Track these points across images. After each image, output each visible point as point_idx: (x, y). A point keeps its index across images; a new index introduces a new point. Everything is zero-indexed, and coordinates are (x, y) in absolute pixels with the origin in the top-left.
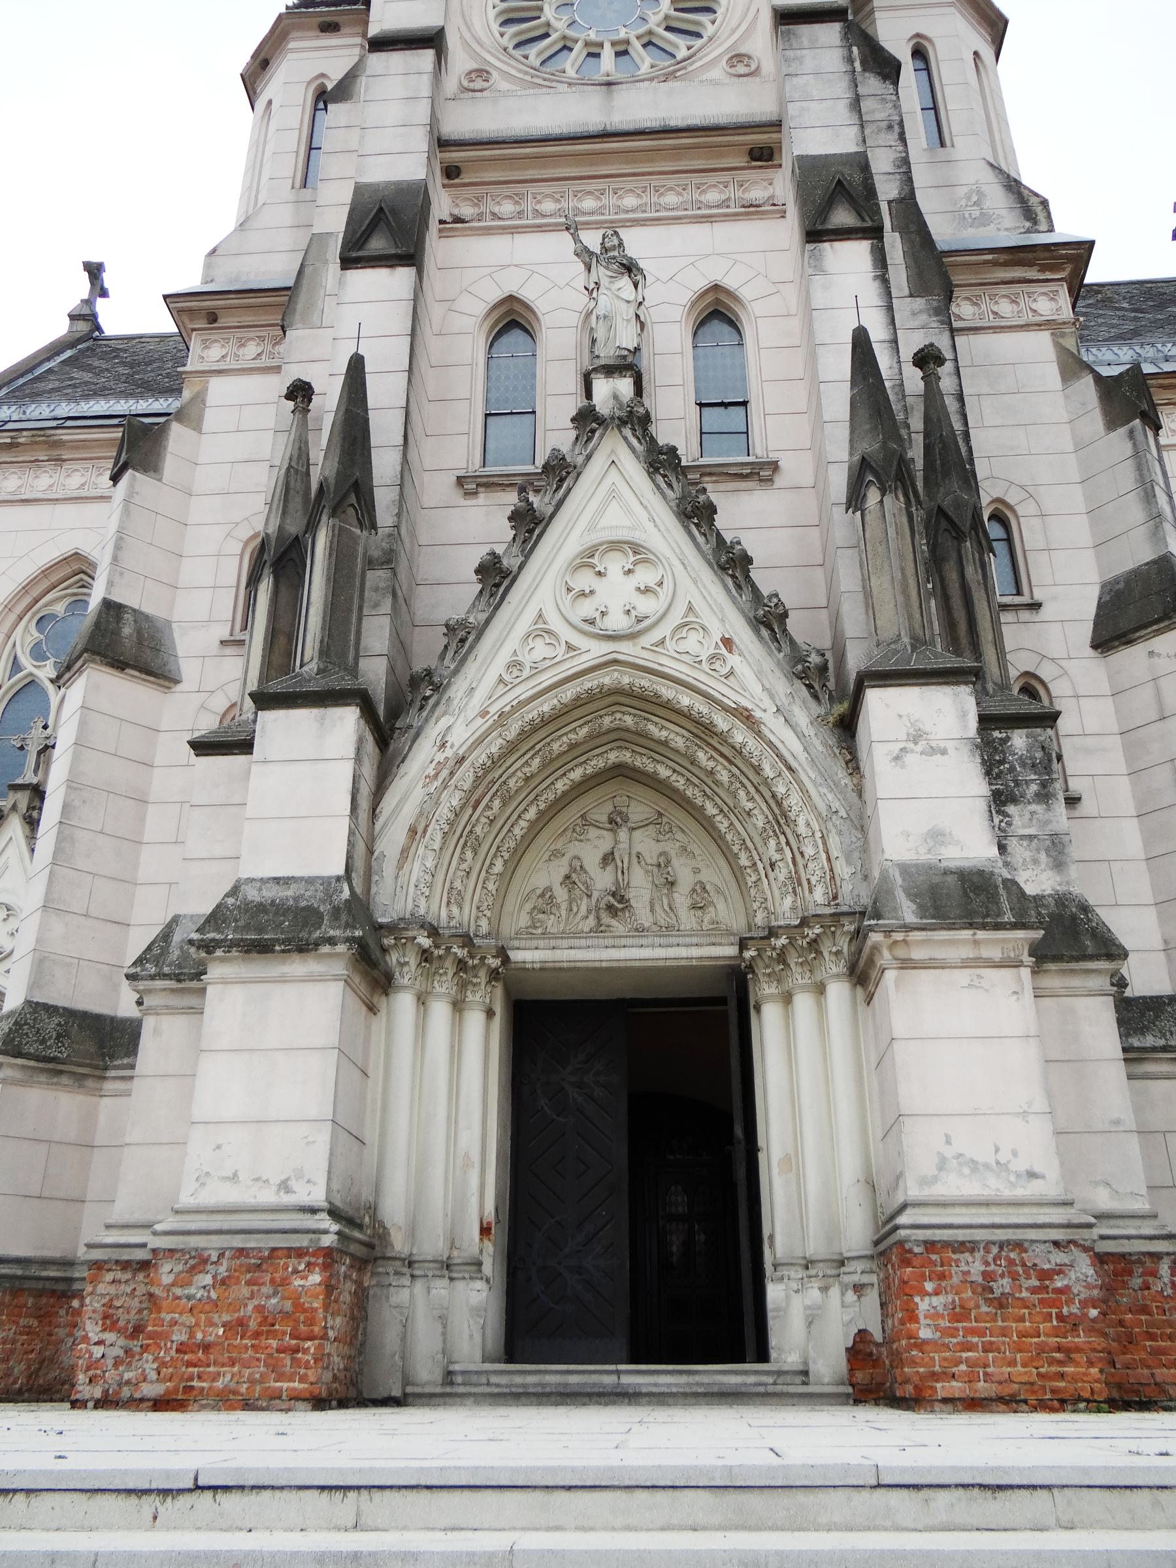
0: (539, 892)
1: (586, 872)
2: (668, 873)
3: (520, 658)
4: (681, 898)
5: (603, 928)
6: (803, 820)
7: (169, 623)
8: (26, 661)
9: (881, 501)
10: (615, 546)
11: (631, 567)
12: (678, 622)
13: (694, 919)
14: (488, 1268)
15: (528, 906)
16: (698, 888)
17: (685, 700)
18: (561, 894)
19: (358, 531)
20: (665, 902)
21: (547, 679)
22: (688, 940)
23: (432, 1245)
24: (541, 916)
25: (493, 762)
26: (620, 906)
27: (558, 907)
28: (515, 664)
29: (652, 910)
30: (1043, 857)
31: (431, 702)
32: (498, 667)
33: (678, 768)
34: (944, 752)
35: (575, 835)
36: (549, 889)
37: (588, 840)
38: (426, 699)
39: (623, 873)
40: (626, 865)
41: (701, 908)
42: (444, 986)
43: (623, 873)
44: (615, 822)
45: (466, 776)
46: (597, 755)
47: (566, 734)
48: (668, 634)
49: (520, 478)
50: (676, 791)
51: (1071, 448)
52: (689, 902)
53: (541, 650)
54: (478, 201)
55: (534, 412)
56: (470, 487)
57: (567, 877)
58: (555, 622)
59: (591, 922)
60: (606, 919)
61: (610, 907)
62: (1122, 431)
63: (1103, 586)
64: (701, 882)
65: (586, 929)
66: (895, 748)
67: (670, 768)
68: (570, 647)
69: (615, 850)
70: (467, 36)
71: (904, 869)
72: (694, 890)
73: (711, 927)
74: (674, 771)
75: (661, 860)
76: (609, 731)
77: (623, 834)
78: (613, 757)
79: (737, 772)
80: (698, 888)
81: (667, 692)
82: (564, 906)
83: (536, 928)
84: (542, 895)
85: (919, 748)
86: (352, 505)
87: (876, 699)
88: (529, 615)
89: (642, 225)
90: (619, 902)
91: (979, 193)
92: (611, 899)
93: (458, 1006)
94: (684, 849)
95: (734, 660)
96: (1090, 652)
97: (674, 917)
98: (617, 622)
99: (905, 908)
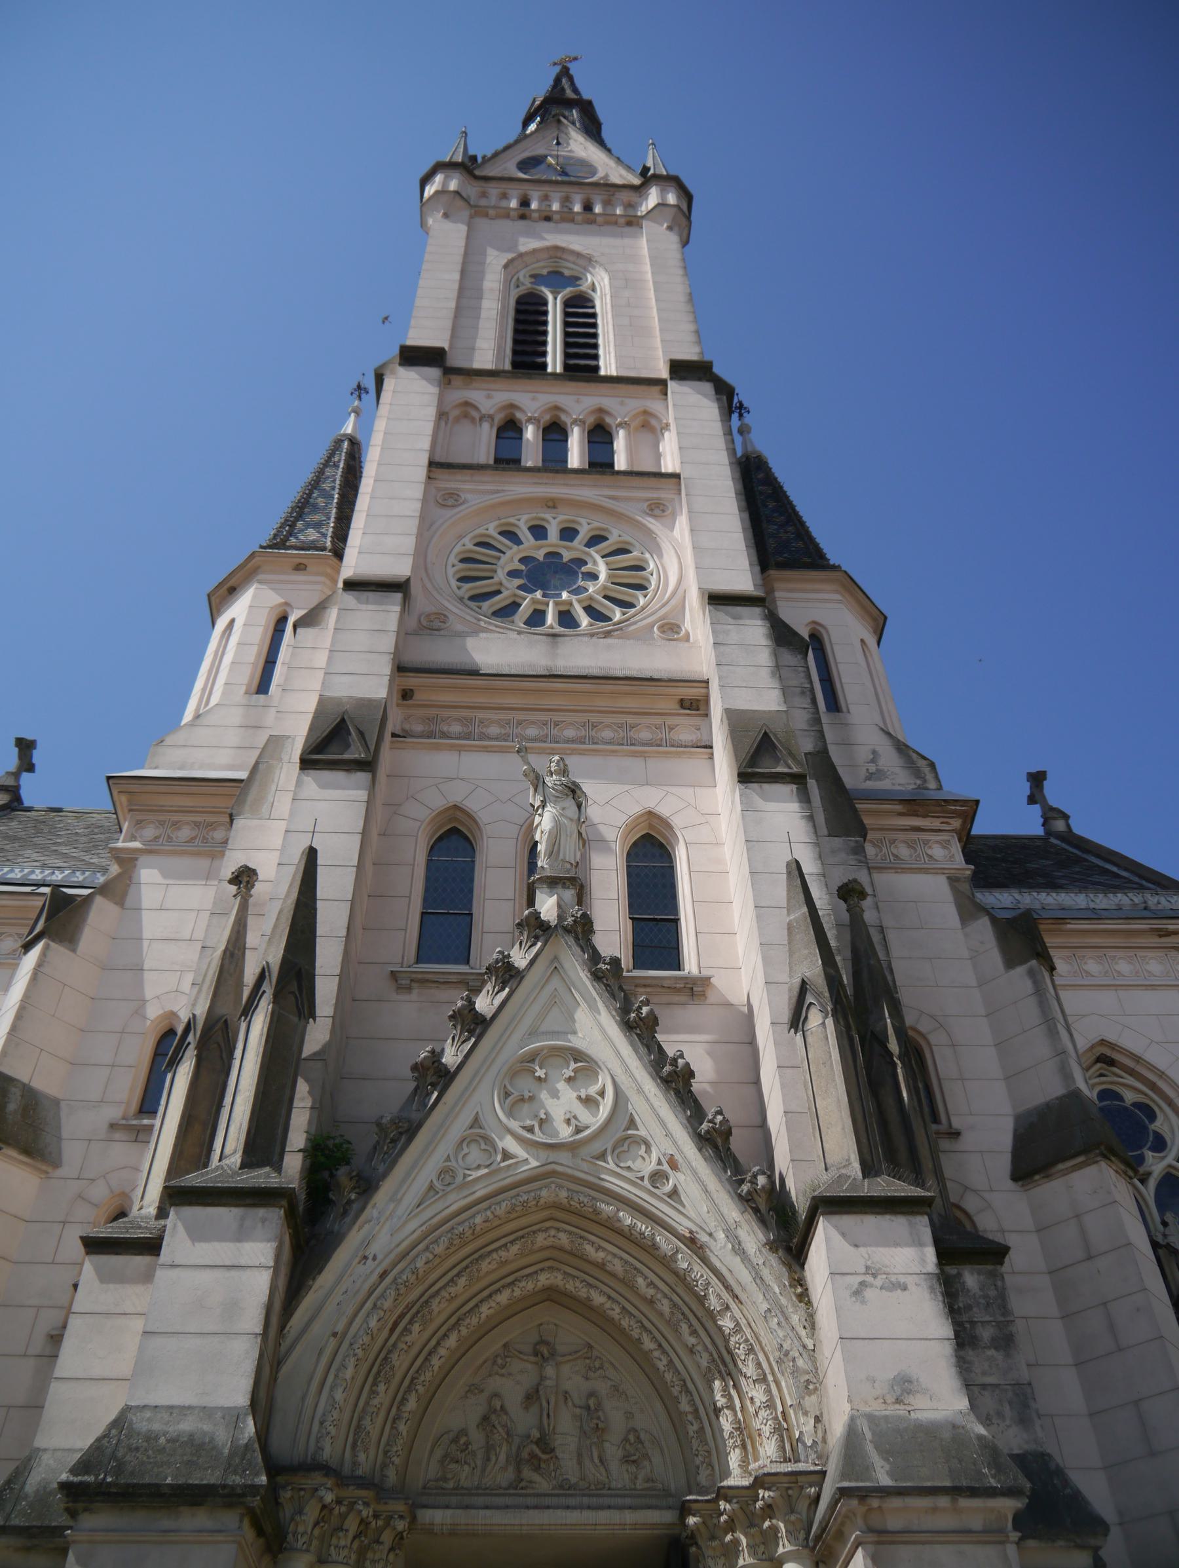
0: (452, 1435)
1: (506, 1413)
2: (599, 1418)
3: (453, 1164)
4: (613, 1452)
5: (523, 1484)
9: (823, 1023)
11: (573, 1074)
12: (619, 1134)
13: (626, 1476)
15: (438, 1453)
16: (632, 1438)
17: (626, 1219)
18: (477, 1438)
19: (296, 1019)
20: (595, 1455)
22: (620, 1501)
24: (453, 1466)
25: (417, 1278)
26: (544, 1457)
27: (474, 1453)
28: (446, 1172)
29: (580, 1463)
30: (1007, 1410)
31: (355, 1206)
32: (428, 1172)
33: (613, 1294)
34: (904, 1288)
35: (496, 1368)
36: (463, 1432)
37: (510, 1374)
38: (350, 1202)
39: (548, 1415)
40: (551, 1406)
41: (634, 1462)
43: (548, 1415)
44: (543, 1351)
46: (527, 1276)
47: (496, 1250)
48: (609, 1146)
49: (455, 977)
50: (611, 1320)
51: (974, 983)
52: (620, 1453)
55: (471, 915)
56: (403, 982)
57: (485, 1418)
59: (510, 1474)
60: (527, 1473)
61: (533, 1456)
62: (1021, 970)
63: (1018, 1118)
64: (634, 1430)
65: (504, 1484)
66: (855, 1281)
67: (605, 1293)
69: (541, 1388)
70: (429, 586)
71: (871, 1418)
72: (626, 1440)
73: (646, 1485)
74: (609, 1297)
75: (592, 1402)
76: (542, 1249)
77: (550, 1371)
78: (544, 1279)
79: (680, 1302)
80: (632, 1438)
82: (480, 1455)
83: (445, 1480)
84: (455, 1440)
85: (879, 1282)
86: (293, 993)
88: (465, 1119)
89: (580, 754)
90: (544, 1452)
91: (874, 752)
92: (534, 1447)
94: (616, 1388)
96: (1010, 1184)
97: (604, 1473)
99: (878, 1469)
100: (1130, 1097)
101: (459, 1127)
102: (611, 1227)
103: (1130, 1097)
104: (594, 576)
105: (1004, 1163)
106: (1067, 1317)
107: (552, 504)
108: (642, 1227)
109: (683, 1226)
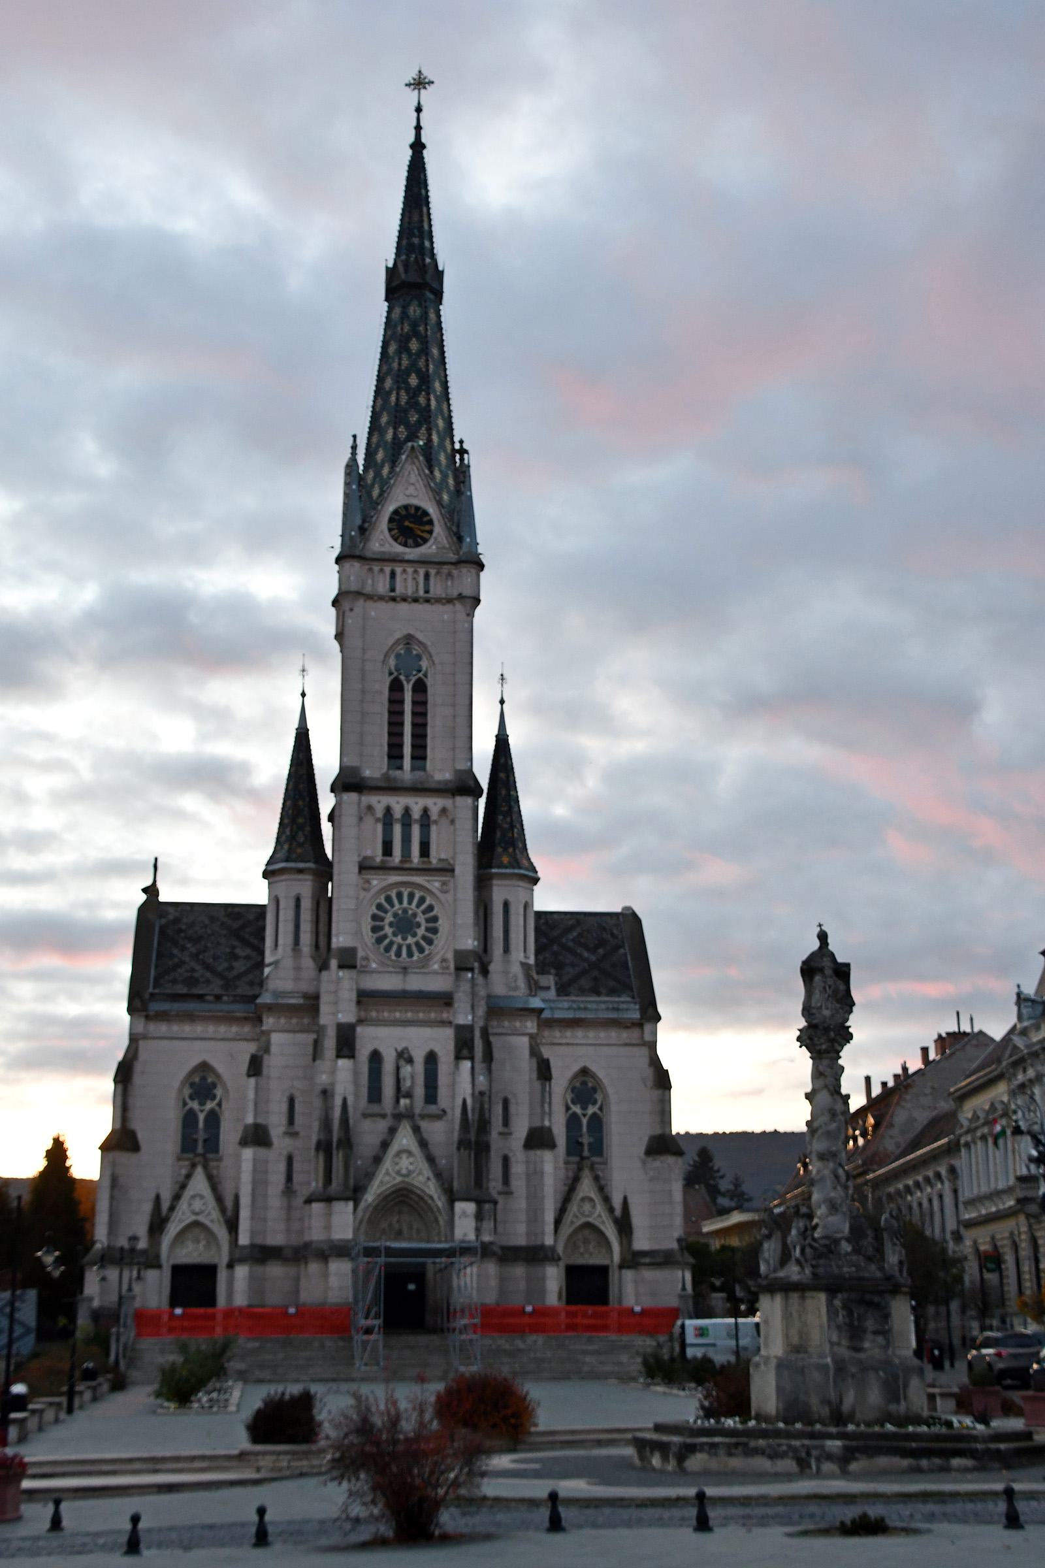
6: (441, 1223)
8: (188, 1100)
17: (419, 1192)
21: (389, 1186)
28: (382, 1182)
44: (400, 1213)
45: (371, 1209)
53: (387, 1178)
58: (390, 1171)
68: (394, 1178)
98: (404, 1171)
100: (590, 1085)
101: (384, 1171)
102: (415, 1193)
103: (590, 1085)
104: (419, 925)
105: (522, 1142)
106: (528, 1186)
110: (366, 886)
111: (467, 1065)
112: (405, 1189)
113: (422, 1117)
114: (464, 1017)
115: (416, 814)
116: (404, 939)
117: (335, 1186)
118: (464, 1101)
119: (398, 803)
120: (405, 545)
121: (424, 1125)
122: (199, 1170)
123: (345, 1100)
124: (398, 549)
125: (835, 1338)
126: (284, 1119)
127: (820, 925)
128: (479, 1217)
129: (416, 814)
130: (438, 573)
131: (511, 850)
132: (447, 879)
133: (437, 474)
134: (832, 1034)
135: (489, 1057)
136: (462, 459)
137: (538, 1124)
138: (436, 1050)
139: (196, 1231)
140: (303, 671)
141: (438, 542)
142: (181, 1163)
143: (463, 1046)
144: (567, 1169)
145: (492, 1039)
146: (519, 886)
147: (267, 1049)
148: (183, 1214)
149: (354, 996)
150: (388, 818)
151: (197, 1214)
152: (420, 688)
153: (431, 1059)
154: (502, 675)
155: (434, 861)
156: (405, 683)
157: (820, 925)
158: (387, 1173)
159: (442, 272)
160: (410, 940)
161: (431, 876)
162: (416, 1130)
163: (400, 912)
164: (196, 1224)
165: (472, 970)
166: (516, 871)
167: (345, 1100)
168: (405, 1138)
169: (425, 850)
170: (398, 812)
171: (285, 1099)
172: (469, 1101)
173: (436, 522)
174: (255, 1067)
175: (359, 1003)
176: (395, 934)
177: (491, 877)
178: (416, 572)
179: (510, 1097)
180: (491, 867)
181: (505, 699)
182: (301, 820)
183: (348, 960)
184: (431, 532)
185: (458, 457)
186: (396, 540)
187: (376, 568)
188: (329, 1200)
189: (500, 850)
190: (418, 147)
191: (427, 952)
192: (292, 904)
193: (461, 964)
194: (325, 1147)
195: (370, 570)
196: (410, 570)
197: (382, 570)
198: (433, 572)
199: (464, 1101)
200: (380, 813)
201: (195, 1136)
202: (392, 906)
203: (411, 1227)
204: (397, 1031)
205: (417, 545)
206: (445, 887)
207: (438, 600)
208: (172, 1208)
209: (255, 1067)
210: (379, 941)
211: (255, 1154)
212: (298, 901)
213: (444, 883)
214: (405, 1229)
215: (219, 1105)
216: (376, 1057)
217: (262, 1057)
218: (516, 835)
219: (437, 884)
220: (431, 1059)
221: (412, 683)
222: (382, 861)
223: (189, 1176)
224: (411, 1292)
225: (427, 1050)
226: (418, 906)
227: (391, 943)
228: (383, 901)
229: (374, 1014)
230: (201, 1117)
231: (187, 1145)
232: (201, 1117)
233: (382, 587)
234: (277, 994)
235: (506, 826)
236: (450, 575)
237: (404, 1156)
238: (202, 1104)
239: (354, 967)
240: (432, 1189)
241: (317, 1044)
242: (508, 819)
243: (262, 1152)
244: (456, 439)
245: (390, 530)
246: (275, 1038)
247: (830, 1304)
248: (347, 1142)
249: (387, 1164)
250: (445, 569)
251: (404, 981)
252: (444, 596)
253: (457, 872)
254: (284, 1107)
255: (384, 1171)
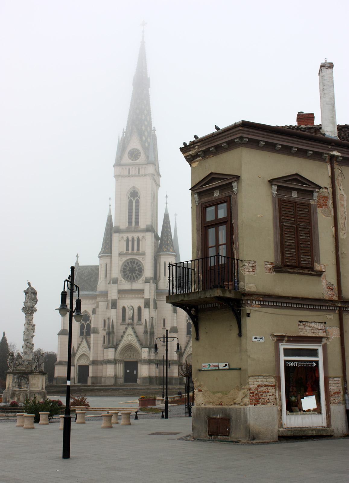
4: (134, 356)
7: (98, 328)
10: (130, 334)
14: (123, 378)
17: (134, 345)
23: (120, 377)
32: (122, 343)
42: (120, 363)
53: (125, 342)
54: (121, 295)
62: (173, 314)
68: (127, 342)
81: (133, 345)
87: (143, 349)
93: (121, 364)
95: (137, 343)
98: (130, 340)
101: (124, 340)
102: (133, 346)
107: (133, 259)
108: (135, 346)
109: (137, 346)
110: (121, 260)
111: (147, 309)
112: (129, 345)
113: (137, 325)
114: (147, 296)
115: (136, 238)
116: (132, 274)
117: (110, 345)
118: (146, 320)
119: (135, 235)
120: (133, 160)
121: (137, 328)
122: (84, 340)
123: (113, 320)
124: (131, 161)
125: (14, 385)
126: (103, 326)
127: (28, 281)
128: (149, 352)
129: (136, 238)
130: (142, 167)
131: (167, 247)
132: (144, 257)
133: (144, 138)
134: (27, 309)
135: (156, 307)
136: (154, 133)
137: (173, 326)
138: (140, 305)
139: (84, 356)
140: (110, 198)
141: (142, 158)
142: (80, 338)
143: (147, 305)
144: (187, 338)
145: (157, 302)
146: (169, 257)
147: (97, 307)
148: (80, 352)
149: (116, 291)
150: (128, 240)
151: (84, 352)
152: (137, 202)
153: (139, 309)
154: (167, 195)
155: (140, 251)
156: (133, 201)
157: (28, 281)
158: (125, 340)
159: (149, 78)
160: (134, 274)
161: (140, 256)
162: (133, 328)
163: (131, 267)
164: (84, 354)
165: (150, 282)
166: (167, 253)
167: (113, 320)
168: (130, 331)
169: (138, 249)
170: (130, 239)
171: (103, 320)
172: (148, 320)
173: (141, 153)
174: (94, 312)
175: (119, 293)
176: (129, 273)
177: (160, 255)
178: (136, 168)
179: (165, 318)
180: (160, 252)
181: (168, 202)
182: (108, 242)
183: (115, 281)
184: (140, 156)
185: (153, 132)
186: (130, 159)
187: (124, 168)
188: (108, 348)
189: (164, 247)
190: (143, 43)
191: (139, 278)
192: (104, 266)
193: (147, 281)
194: (109, 334)
195: (123, 168)
196: (134, 168)
197: (126, 168)
198: (140, 167)
199: (146, 320)
200: (125, 238)
201: (83, 331)
202: (129, 265)
203: (133, 355)
204: (130, 301)
205: (136, 160)
206: (143, 259)
207: (142, 175)
208: (77, 350)
209: (94, 312)
210: (125, 275)
211: (94, 335)
212: (106, 265)
213: (143, 258)
214: (132, 355)
215: (90, 322)
216: (124, 309)
217: (96, 309)
218: (168, 243)
219: (141, 258)
220: (139, 309)
221: (135, 201)
222: (126, 252)
223: (81, 342)
224: (128, 372)
225: (138, 306)
226: (136, 265)
227: (129, 276)
228: (126, 264)
229: (123, 296)
230: (85, 325)
231: (82, 333)
232: (85, 325)
233: (127, 173)
234: (100, 292)
235: (166, 240)
236: (145, 167)
237: (130, 336)
238: (86, 322)
239: (117, 283)
240: (137, 345)
241: (108, 305)
242: (167, 238)
243: (96, 335)
244: (153, 126)
245: (128, 156)
246: (100, 304)
247: (13, 377)
248: (113, 332)
249: (125, 338)
250: (144, 166)
251: (132, 286)
252: (144, 174)
253: (146, 255)
254: (103, 323)
255: (124, 340)
